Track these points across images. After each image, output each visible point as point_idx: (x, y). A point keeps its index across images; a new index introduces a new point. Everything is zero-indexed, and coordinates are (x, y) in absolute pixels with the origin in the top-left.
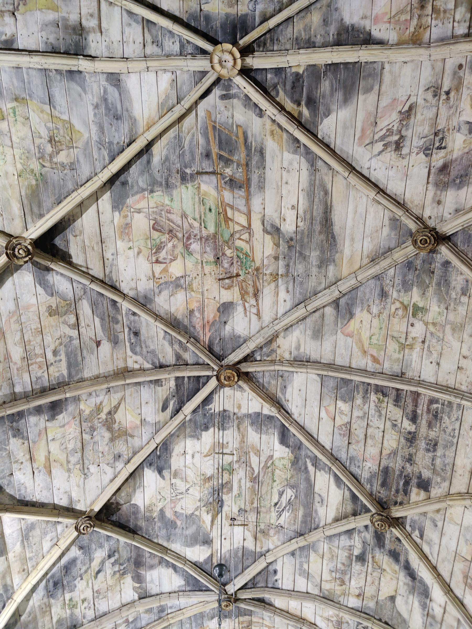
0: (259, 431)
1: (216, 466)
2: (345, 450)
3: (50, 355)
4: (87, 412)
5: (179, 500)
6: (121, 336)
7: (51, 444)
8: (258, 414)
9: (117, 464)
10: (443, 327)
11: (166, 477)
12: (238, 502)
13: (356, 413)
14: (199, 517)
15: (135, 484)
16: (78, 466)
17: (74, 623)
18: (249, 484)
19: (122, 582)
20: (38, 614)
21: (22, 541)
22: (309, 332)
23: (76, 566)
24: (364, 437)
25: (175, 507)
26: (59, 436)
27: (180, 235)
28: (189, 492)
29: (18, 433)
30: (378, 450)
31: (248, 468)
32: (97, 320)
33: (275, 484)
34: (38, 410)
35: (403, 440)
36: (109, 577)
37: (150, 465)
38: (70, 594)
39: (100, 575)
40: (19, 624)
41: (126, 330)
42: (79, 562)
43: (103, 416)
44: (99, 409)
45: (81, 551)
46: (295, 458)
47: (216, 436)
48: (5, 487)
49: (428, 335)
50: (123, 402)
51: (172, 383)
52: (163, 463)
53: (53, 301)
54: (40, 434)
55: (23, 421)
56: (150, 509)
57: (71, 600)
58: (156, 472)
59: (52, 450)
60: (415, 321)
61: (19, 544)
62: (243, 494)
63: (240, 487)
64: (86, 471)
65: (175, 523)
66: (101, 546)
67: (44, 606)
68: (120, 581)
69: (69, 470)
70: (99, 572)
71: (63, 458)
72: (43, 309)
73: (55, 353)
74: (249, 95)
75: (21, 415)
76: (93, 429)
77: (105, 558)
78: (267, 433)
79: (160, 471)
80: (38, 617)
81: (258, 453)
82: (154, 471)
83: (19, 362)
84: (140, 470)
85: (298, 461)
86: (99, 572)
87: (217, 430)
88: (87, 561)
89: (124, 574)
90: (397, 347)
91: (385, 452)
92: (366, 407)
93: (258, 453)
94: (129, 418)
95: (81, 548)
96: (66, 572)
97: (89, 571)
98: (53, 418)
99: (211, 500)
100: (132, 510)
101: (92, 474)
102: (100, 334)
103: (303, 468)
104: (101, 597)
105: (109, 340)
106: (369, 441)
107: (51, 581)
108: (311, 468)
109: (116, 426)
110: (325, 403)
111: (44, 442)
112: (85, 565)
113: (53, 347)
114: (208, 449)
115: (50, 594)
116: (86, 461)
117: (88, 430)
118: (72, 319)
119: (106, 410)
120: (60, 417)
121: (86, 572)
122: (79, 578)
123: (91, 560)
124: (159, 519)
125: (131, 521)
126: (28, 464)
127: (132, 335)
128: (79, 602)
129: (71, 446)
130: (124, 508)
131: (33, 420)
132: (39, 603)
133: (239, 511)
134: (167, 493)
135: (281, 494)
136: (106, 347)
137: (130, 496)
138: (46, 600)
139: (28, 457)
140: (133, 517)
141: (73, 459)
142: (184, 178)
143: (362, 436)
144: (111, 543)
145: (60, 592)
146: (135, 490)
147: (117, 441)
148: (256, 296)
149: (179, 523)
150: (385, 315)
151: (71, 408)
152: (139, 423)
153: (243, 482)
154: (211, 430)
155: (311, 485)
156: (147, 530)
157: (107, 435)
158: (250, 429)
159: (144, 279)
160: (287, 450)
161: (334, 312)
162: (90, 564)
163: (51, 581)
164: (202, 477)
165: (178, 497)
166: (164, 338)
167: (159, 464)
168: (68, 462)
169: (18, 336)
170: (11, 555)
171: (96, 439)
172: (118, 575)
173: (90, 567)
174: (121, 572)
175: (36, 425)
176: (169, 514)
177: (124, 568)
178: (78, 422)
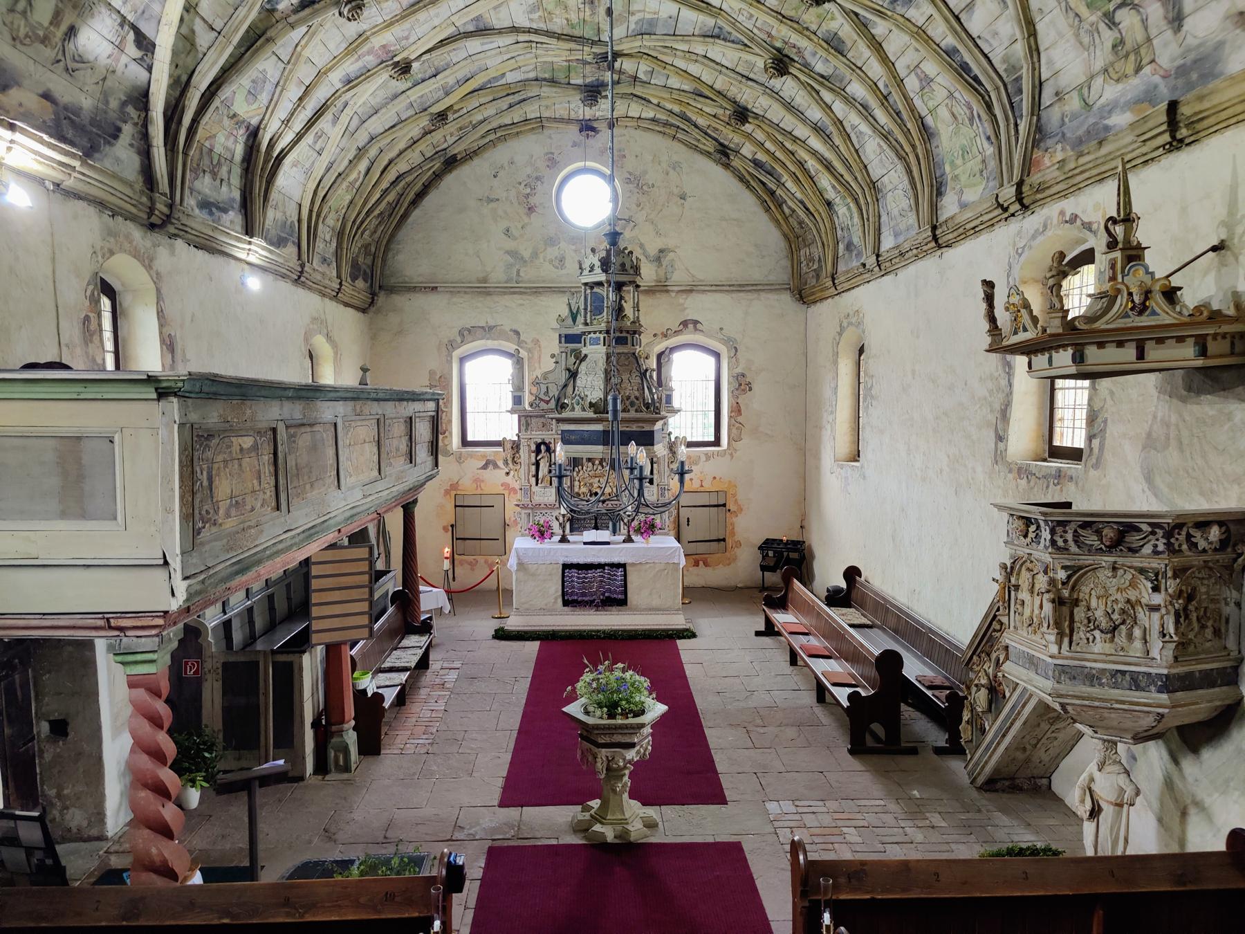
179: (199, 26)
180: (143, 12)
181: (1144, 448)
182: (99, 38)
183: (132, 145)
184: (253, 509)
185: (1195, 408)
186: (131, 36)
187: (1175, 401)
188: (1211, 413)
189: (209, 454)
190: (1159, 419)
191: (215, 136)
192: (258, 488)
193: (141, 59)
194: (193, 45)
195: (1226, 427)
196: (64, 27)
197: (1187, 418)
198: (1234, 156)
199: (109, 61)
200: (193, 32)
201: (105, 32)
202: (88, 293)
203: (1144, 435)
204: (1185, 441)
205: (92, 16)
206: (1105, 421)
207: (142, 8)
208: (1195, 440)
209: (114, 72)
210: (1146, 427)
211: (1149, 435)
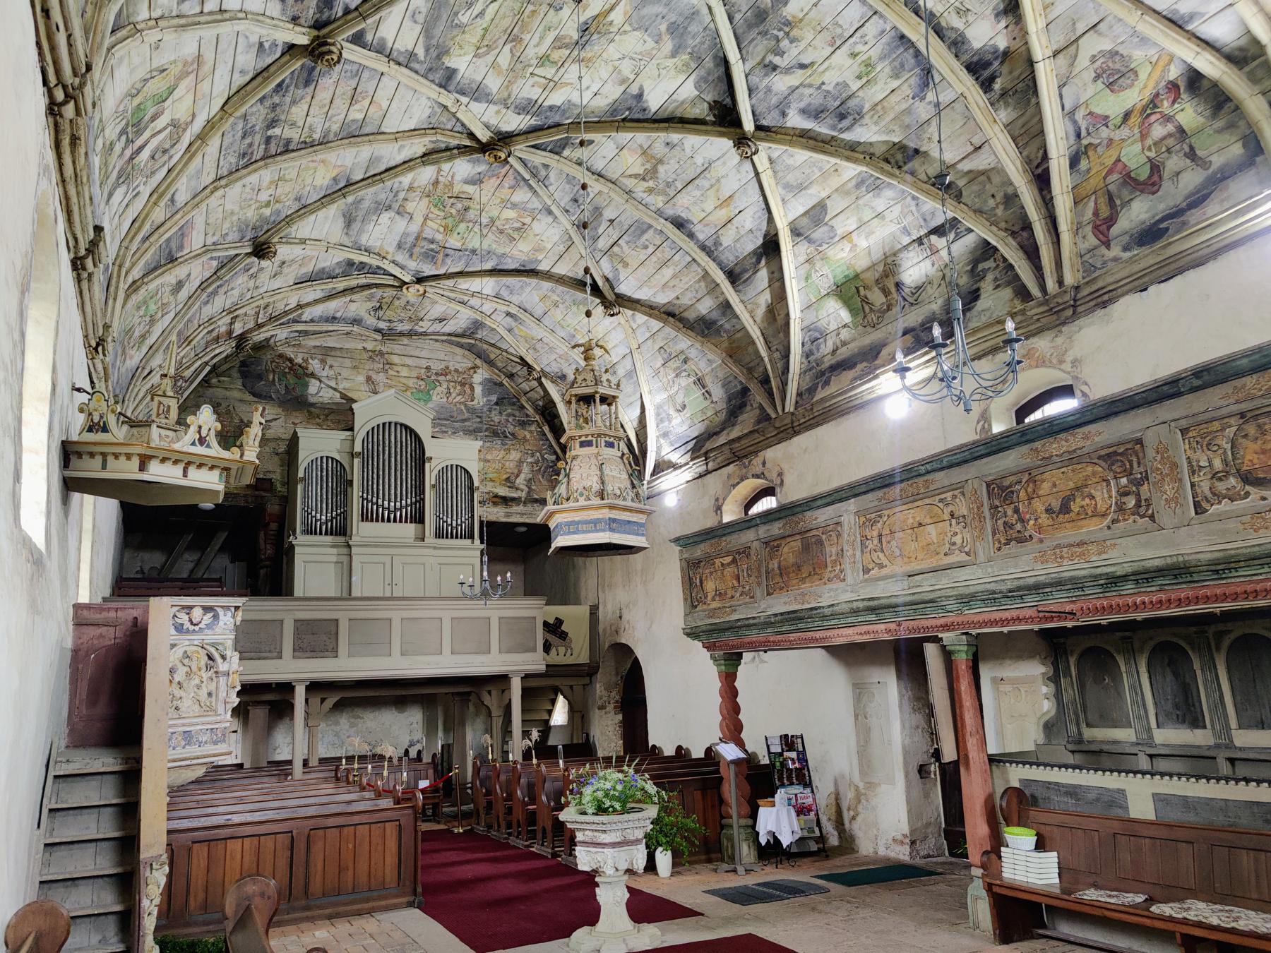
0: (482, 86)
1: (563, 70)
2: (363, 80)
3: (651, 249)
4: (660, 198)
5: (641, 53)
6: (591, 208)
7: (708, 211)
8: (476, 100)
9: (676, 141)
10: (241, 208)
11: (638, 86)
12: (556, 20)
13: (343, 116)
14: (628, 19)
15: (677, 107)
16: (708, 176)
17: (898, 42)
18: (526, 37)
19: (801, 15)
20: (888, 119)
21: (805, 188)
22: (385, 160)
23: (809, 104)
24: (334, 102)
25: (653, 48)
26: (697, 208)
27: (494, 228)
28: (621, 56)
29: (717, 243)
30: (317, 98)
31: (518, 54)
32: (600, 231)
33: (484, 26)
34: (691, 235)
35: (283, 117)
36: (803, 45)
37: (645, 110)
38: (850, 84)
39: (806, 62)
40: (904, 142)
41: (582, 207)
42: (802, 105)
43: (651, 184)
44: (650, 191)
45: (787, 111)
46: (440, 59)
47: (543, 97)
48: (763, 232)
49: (255, 197)
50: (626, 174)
51: (566, 153)
52: (630, 102)
53: (620, 267)
54: (707, 225)
55: (706, 243)
56: (685, 68)
57: (859, 77)
58: (645, 97)
59: (712, 207)
60: (269, 199)
61: (809, 192)
62: (540, 29)
63: (541, 38)
64: (706, 166)
65: (668, 30)
66: (769, 90)
67: (876, 117)
68: (801, 20)
69: (718, 181)
70: (803, 66)
71: (711, 193)
72: (630, 270)
73: (646, 247)
74: (400, 270)
75: (703, 248)
76: (668, 185)
77: (781, 73)
78: (472, 81)
79: (640, 96)
80: (892, 116)
81: (494, 65)
82: (647, 101)
83: (672, 267)
84: (659, 116)
85: (438, 56)
86: (803, 66)
87: (540, 102)
88: (795, 95)
89: (788, 23)
90: (287, 177)
91: (310, 98)
92: (327, 125)
93: (494, 65)
94: (630, 161)
95: (784, 114)
96: (822, 111)
97: (807, 81)
98: (688, 221)
99: (595, 36)
100: (704, 86)
101: (704, 158)
102: (605, 224)
103: (432, 50)
104: (839, 31)
105: (601, 215)
106: (328, 101)
107: (840, 126)
108: (420, 52)
109: (648, 166)
110: (381, 113)
111: (710, 218)
112: (802, 95)
113: (644, 251)
114: (563, 90)
115: (858, 117)
116: (699, 172)
117: (673, 188)
118: (615, 249)
119: (645, 185)
120: (683, 215)
121: (810, 86)
122: (824, 87)
123: (794, 90)
124: (686, 47)
125: (716, 75)
126: (734, 221)
127: (580, 202)
128: (859, 61)
129: (698, 193)
130: (709, 98)
131: (701, 237)
132: (873, 126)
133: (561, 8)
134: (651, 69)
135: (482, 13)
136: (609, 214)
137: (693, 103)
138: (867, 119)
139: (729, 225)
140: (711, 78)
141: (706, 184)
142: (474, 251)
143: (337, 102)
144: (758, 80)
145: (852, 103)
146: (683, 103)
147: (658, 156)
148: (437, 182)
149: (663, 27)
150: (298, 188)
151: (670, 212)
152: (625, 151)
153: (534, 41)
154: (546, 104)
155: (427, 31)
156: (711, 48)
157: (661, 169)
158: (495, 91)
159: (543, 223)
160: (449, 65)
161: (352, 177)
162: (797, 88)
163: (840, 126)
164: (590, 65)
165: (640, 57)
166: (551, 184)
167: (635, 103)
168: (712, 186)
169: (656, 276)
170: (824, 195)
171: (674, 176)
172: (794, 33)
173: (801, 84)
174: (787, 29)
175: (703, 232)
176: (668, 45)
177: (780, 30)
178: (675, 200)
179: (965, 166)
180: (925, 220)
182: (917, 268)
183: (997, 287)
184: (733, 597)
186: (933, 238)
189: (700, 570)
191: (1118, 160)
192: (736, 584)
193: (957, 234)
194: (983, 173)
196: (893, 290)
199: (936, 266)
200: (970, 171)
201: (915, 261)
202: (978, 431)
205: (900, 265)
207: (921, 220)
209: (946, 266)
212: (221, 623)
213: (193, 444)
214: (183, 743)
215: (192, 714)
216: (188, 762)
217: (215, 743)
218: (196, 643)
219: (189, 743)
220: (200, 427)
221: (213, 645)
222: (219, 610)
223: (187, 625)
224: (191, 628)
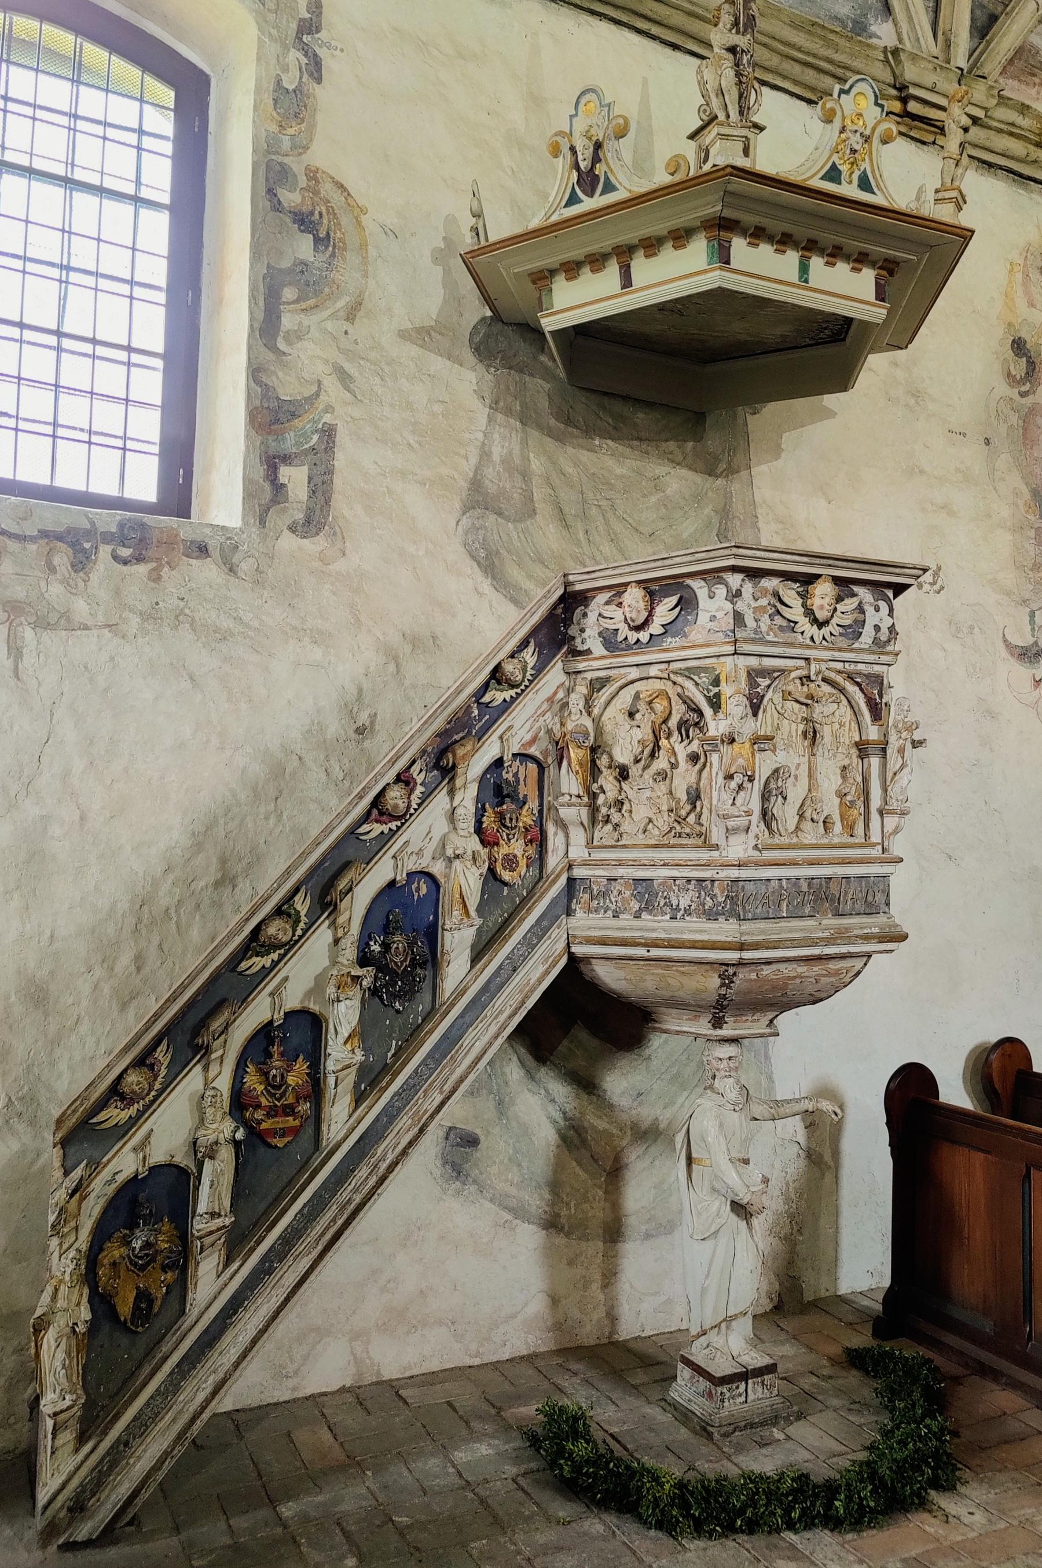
181: (466, 509)
185: (584, 456)
187: (535, 434)
188: (619, 471)
190: (496, 457)
195: (653, 499)
197: (570, 470)
198: (645, 81)
203: (463, 484)
204: (571, 510)
206: (329, 433)
208: (594, 511)
210: (467, 467)
211: (476, 484)
212: (703, 618)
213: (573, 200)
214: (635, 905)
215: (641, 839)
216: (641, 952)
217: (711, 915)
218: (654, 671)
219: (648, 907)
220: (573, 149)
221: (689, 673)
222: (696, 584)
223: (624, 631)
224: (633, 637)
